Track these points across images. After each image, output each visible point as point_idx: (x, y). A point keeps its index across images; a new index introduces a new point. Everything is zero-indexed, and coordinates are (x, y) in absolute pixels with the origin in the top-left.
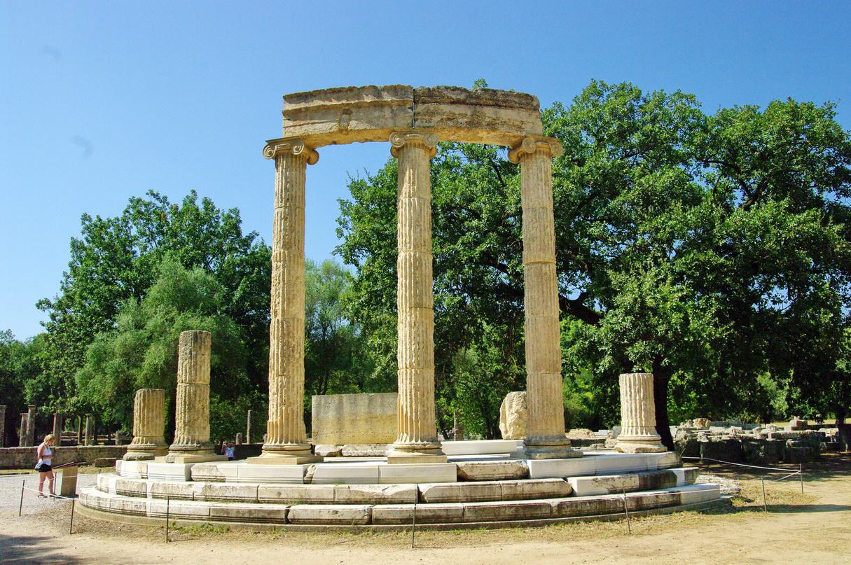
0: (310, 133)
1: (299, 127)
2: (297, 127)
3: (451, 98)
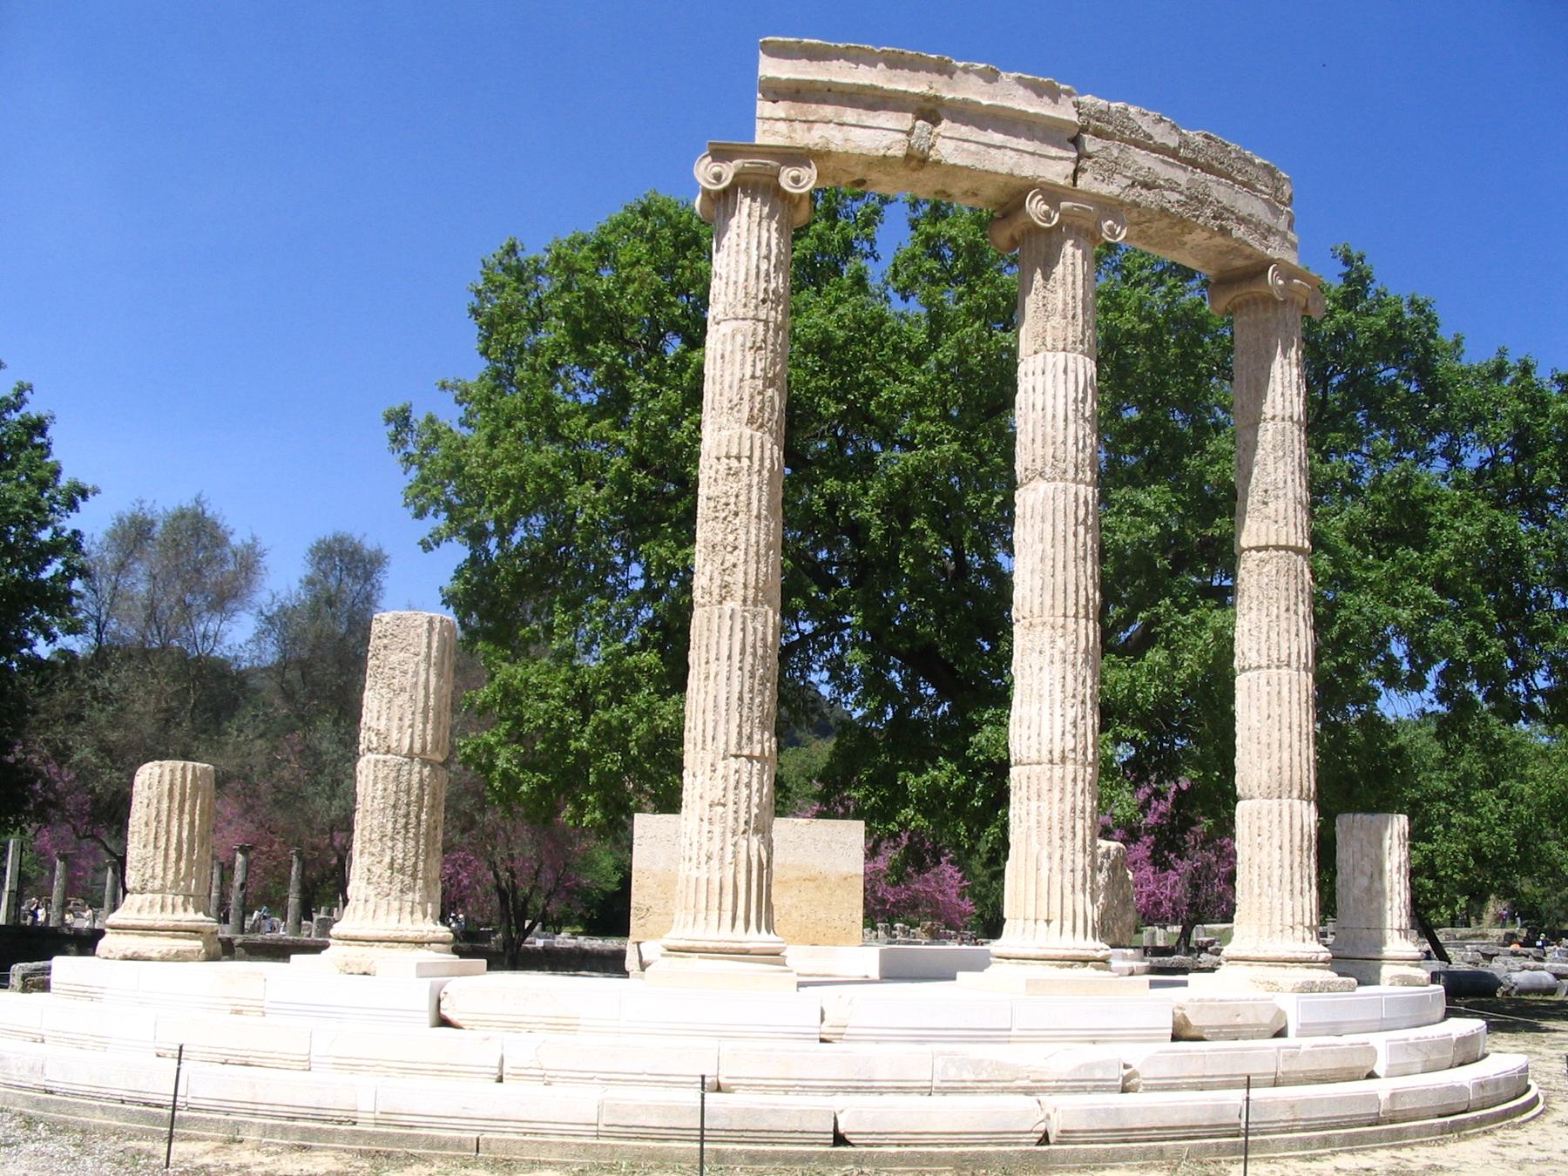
0: (833, 147)
1: (805, 126)
2: (796, 125)
3: (1151, 138)
